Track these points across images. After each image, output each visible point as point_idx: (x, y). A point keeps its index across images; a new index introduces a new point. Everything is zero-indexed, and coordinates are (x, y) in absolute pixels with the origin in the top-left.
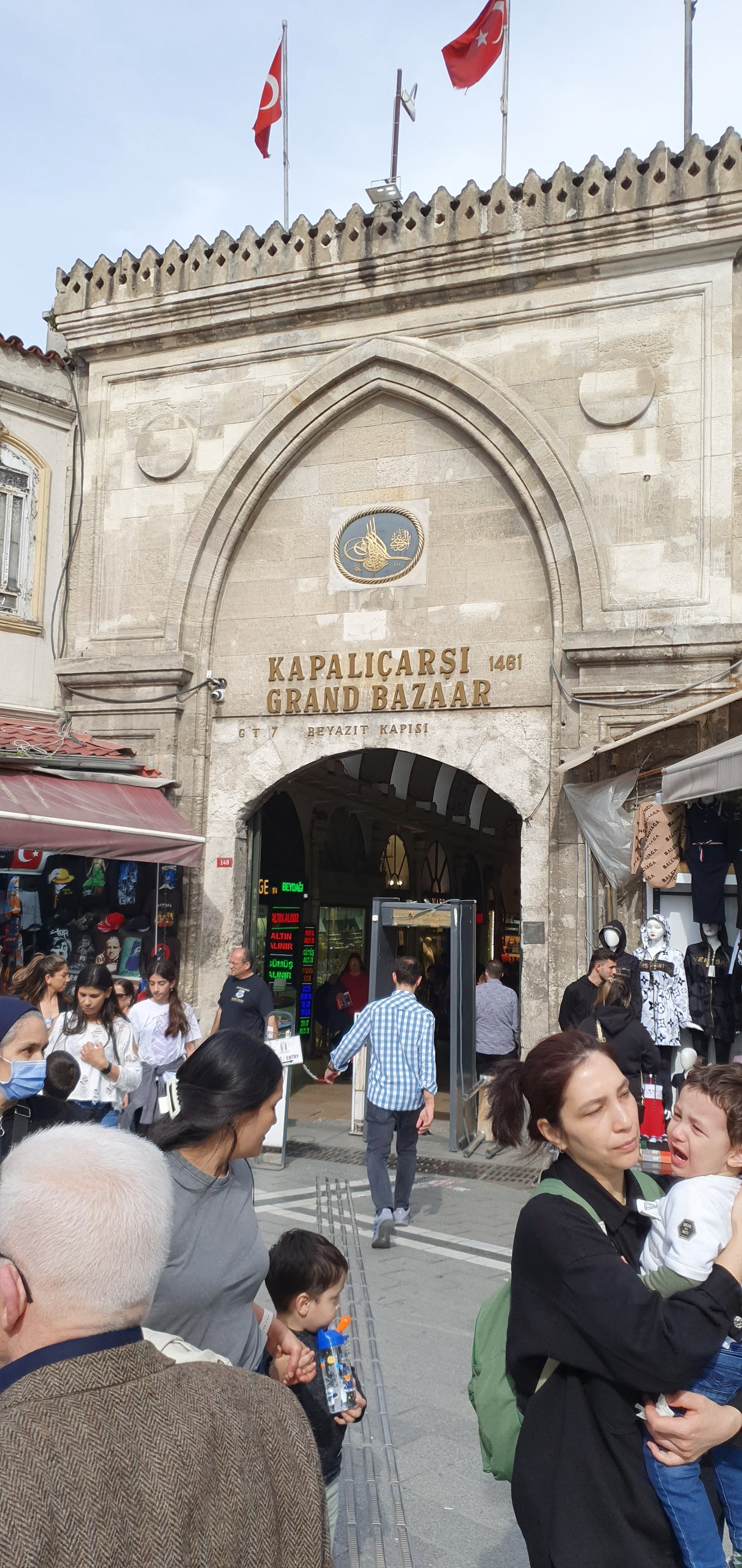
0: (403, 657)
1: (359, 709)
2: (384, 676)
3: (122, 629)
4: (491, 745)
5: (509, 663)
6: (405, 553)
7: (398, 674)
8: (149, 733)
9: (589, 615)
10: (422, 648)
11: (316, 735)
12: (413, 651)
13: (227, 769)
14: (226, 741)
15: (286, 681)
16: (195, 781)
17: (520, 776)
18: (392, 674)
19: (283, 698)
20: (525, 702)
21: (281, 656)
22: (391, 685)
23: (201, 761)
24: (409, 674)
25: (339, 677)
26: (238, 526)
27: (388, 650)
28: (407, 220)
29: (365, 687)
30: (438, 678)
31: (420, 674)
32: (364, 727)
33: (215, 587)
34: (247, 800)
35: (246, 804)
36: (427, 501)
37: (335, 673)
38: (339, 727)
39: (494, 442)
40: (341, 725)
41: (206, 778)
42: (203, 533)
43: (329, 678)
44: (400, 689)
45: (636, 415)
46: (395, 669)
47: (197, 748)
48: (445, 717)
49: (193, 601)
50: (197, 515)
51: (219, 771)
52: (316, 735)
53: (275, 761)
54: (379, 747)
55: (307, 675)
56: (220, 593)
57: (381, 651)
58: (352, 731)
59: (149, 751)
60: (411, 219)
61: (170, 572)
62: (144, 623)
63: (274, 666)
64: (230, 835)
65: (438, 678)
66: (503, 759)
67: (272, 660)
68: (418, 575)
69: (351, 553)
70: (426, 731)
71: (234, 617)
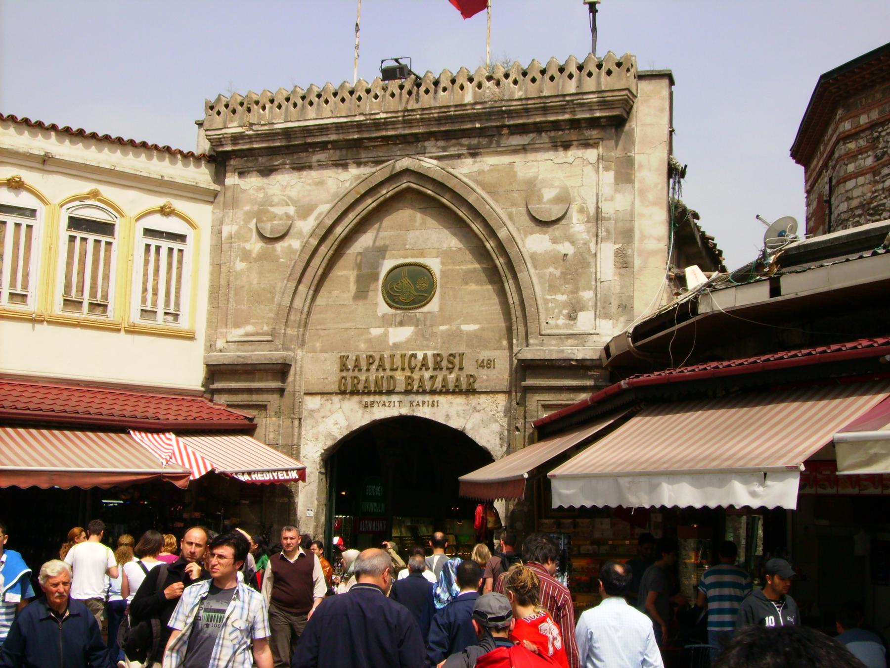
0: (424, 358)
1: (397, 390)
2: (412, 369)
3: (247, 335)
4: (476, 414)
5: (488, 364)
6: (425, 291)
7: (421, 369)
8: (264, 403)
9: (531, 337)
10: (435, 352)
11: (369, 406)
12: (430, 353)
13: (313, 427)
14: (313, 409)
15: (351, 371)
16: (293, 435)
17: (494, 435)
18: (417, 368)
19: (349, 380)
20: (497, 389)
21: (348, 354)
22: (416, 376)
23: (296, 423)
24: (427, 369)
25: (384, 370)
26: (320, 271)
27: (414, 352)
28: (425, 89)
29: (400, 376)
30: (445, 372)
31: (435, 369)
32: (400, 402)
33: (306, 309)
34: (326, 448)
35: (325, 450)
36: (439, 258)
37: (381, 366)
38: (384, 402)
39: (476, 227)
40: (386, 400)
41: (300, 434)
42: (299, 275)
43: (378, 370)
44: (421, 380)
45: (560, 215)
46: (419, 365)
47: (294, 413)
48: (450, 397)
49: (292, 317)
50: (295, 263)
51: (308, 428)
52: (369, 406)
53: (343, 423)
54: (409, 414)
55: (365, 368)
56: (309, 313)
57: (410, 353)
58: (392, 404)
59: (262, 416)
60: (427, 88)
61: (277, 299)
62: (261, 331)
63: (343, 360)
64: (315, 470)
65: (445, 372)
66: (485, 423)
67: (342, 357)
68: (433, 306)
69: (392, 288)
70: (438, 406)
71: (319, 327)
